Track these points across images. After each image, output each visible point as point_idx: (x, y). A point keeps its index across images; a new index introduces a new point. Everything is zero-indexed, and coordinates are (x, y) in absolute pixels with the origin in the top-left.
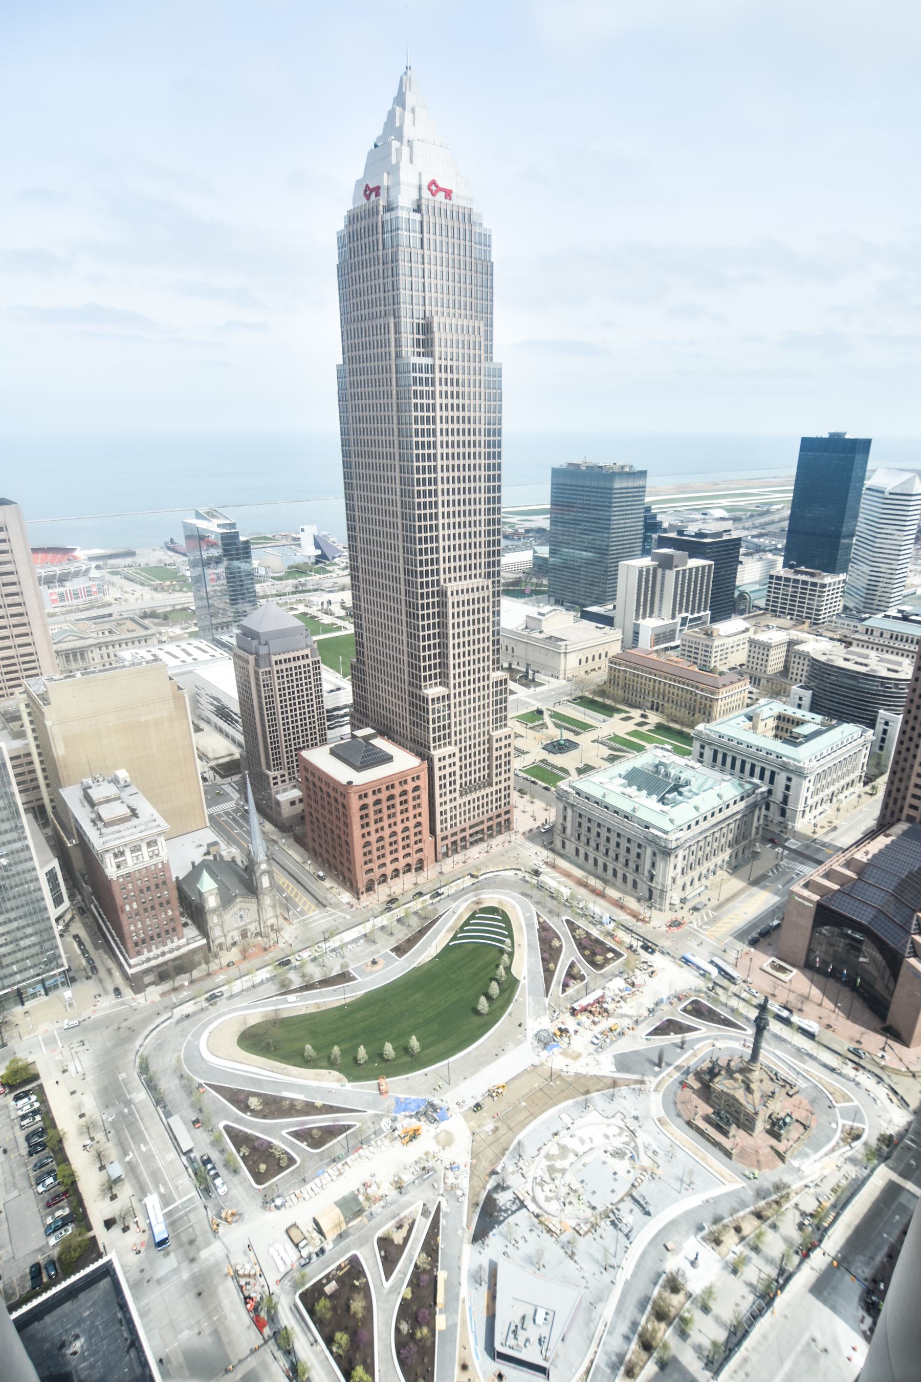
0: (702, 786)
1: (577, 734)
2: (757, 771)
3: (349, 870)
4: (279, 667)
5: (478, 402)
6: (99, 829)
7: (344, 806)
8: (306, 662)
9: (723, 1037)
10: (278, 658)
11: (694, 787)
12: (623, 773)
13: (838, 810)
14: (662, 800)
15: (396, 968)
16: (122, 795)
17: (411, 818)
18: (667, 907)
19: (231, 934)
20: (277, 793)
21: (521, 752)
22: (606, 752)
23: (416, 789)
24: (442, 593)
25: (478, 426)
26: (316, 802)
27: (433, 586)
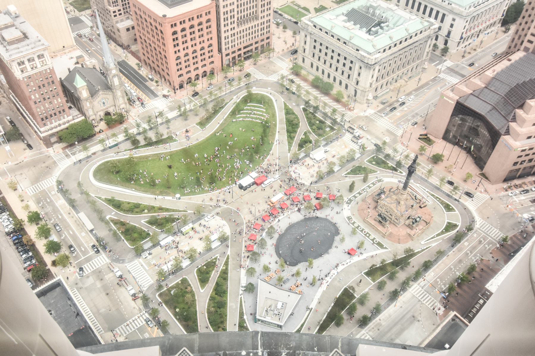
0: (396, 23)
2: (434, 13)
3: (168, 74)
6: (5, 47)
7: (162, 32)
9: (387, 177)
12: (345, 12)
13: (482, 42)
16: (15, 23)
17: (206, 41)
18: (365, 101)
19: (99, 113)
20: (117, 22)
23: (208, 21)
26: (143, 29)
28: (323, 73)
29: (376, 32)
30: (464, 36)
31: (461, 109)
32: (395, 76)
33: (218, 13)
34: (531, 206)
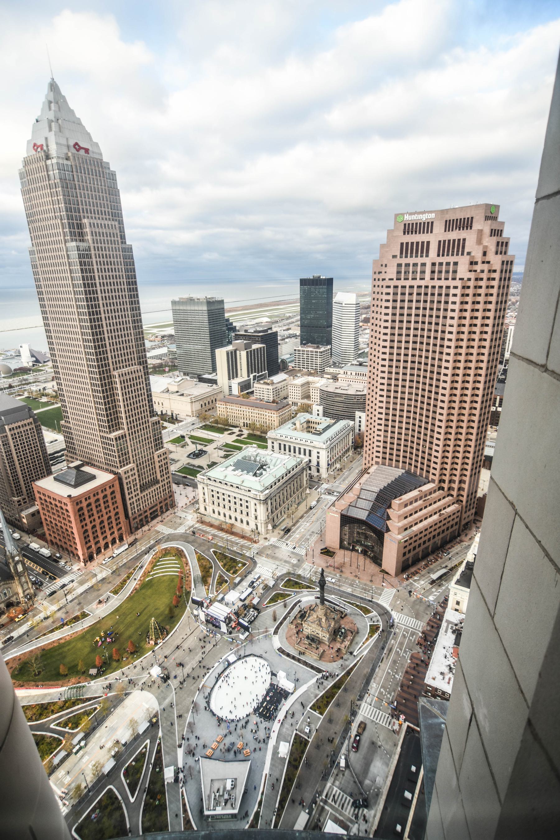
4: (13, 432)
7: (67, 511)
8: (31, 427)
10: (11, 426)
12: (232, 464)
14: (255, 475)
20: (22, 510)
22: (222, 453)
23: (113, 492)
28: (225, 516)
29: (261, 474)
30: (330, 462)
31: (346, 520)
32: (286, 505)
33: (121, 484)
34: (432, 588)
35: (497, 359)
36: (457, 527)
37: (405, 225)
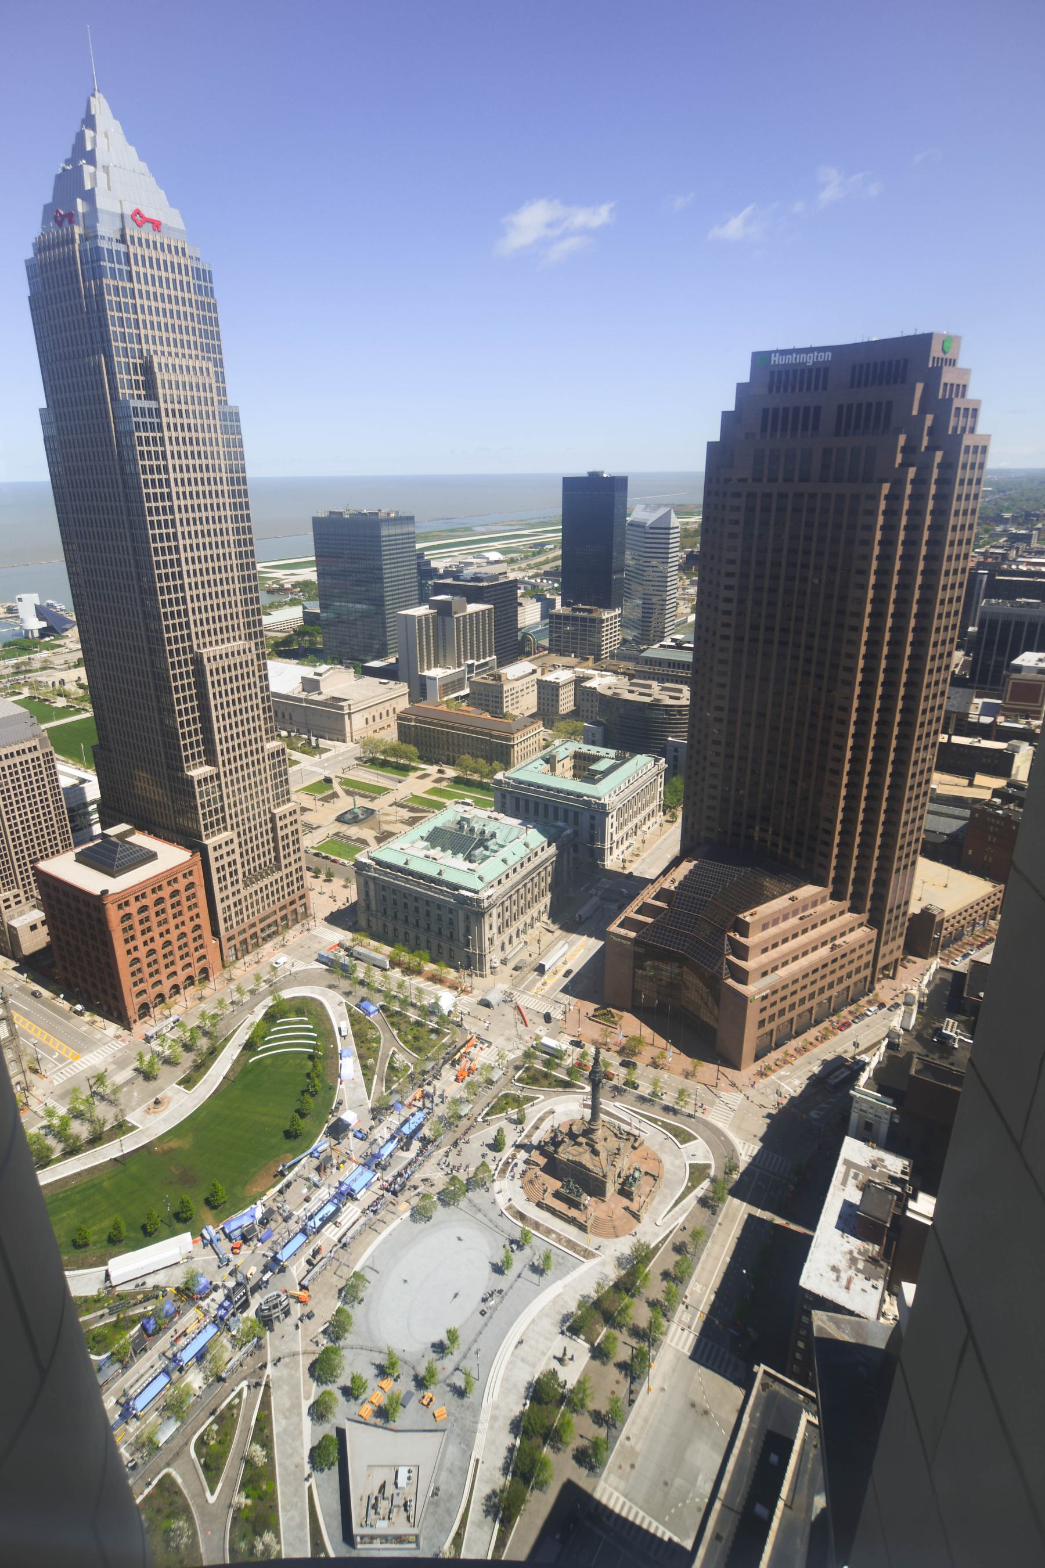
1: (373, 799)
5: (215, 449)
11: (499, 839)
12: (425, 835)
14: (470, 859)
15: (182, 1103)
18: (488, 971)
21: (310, 828)
23: (190, 886)
24: (198, 661)
25: (218, 475)
27: (185, 653)
35: (952, 640)
36: (868, 972)
37: (772, 373)
